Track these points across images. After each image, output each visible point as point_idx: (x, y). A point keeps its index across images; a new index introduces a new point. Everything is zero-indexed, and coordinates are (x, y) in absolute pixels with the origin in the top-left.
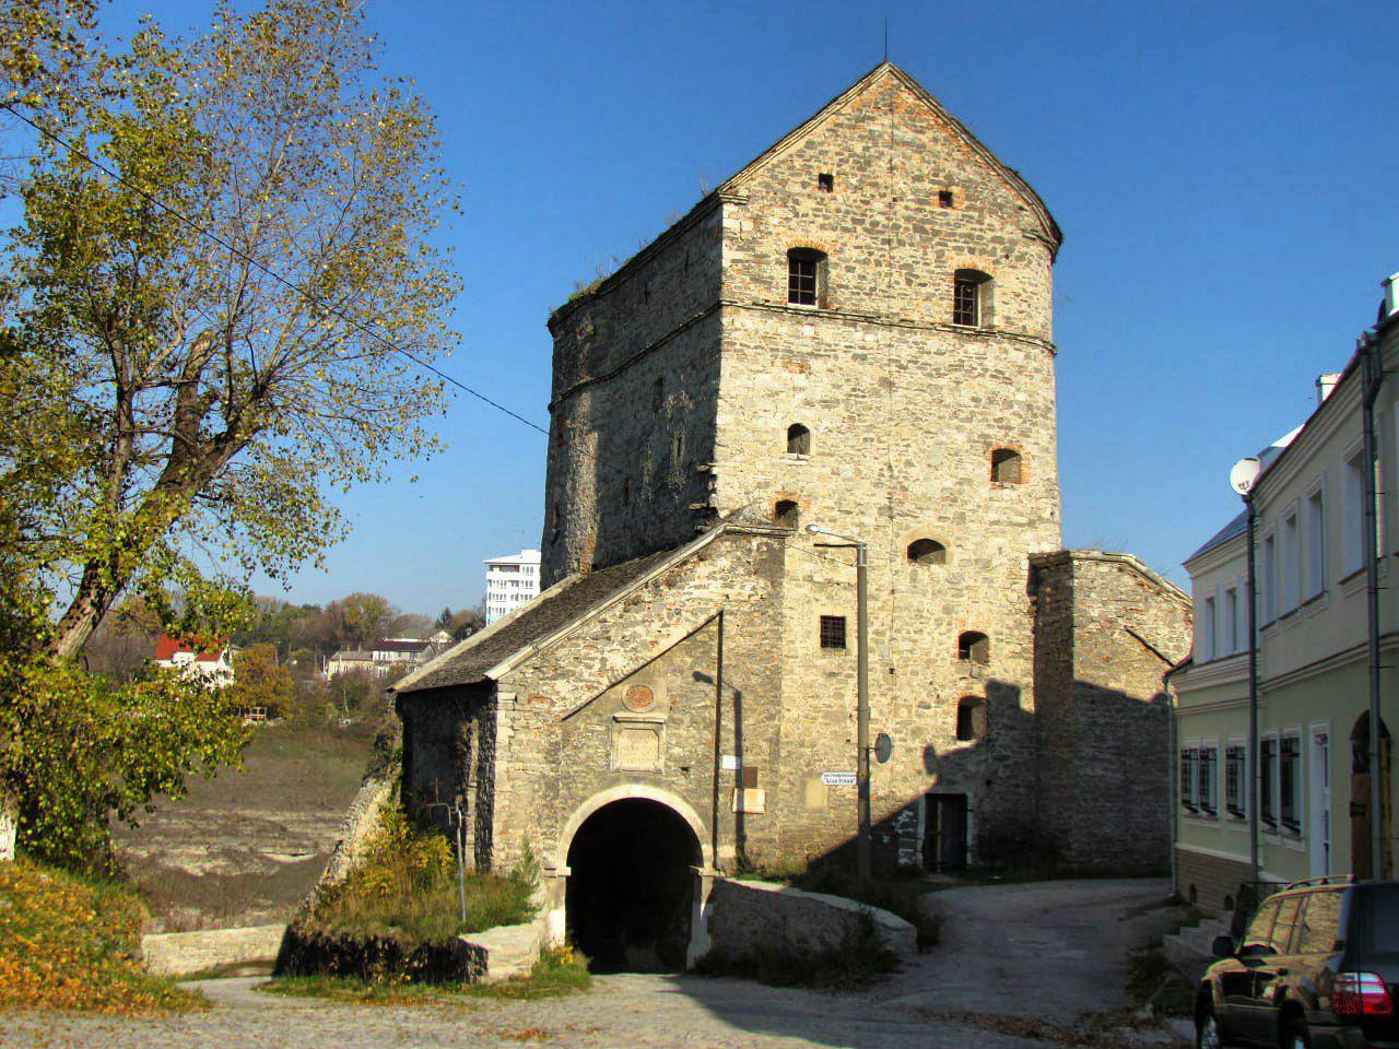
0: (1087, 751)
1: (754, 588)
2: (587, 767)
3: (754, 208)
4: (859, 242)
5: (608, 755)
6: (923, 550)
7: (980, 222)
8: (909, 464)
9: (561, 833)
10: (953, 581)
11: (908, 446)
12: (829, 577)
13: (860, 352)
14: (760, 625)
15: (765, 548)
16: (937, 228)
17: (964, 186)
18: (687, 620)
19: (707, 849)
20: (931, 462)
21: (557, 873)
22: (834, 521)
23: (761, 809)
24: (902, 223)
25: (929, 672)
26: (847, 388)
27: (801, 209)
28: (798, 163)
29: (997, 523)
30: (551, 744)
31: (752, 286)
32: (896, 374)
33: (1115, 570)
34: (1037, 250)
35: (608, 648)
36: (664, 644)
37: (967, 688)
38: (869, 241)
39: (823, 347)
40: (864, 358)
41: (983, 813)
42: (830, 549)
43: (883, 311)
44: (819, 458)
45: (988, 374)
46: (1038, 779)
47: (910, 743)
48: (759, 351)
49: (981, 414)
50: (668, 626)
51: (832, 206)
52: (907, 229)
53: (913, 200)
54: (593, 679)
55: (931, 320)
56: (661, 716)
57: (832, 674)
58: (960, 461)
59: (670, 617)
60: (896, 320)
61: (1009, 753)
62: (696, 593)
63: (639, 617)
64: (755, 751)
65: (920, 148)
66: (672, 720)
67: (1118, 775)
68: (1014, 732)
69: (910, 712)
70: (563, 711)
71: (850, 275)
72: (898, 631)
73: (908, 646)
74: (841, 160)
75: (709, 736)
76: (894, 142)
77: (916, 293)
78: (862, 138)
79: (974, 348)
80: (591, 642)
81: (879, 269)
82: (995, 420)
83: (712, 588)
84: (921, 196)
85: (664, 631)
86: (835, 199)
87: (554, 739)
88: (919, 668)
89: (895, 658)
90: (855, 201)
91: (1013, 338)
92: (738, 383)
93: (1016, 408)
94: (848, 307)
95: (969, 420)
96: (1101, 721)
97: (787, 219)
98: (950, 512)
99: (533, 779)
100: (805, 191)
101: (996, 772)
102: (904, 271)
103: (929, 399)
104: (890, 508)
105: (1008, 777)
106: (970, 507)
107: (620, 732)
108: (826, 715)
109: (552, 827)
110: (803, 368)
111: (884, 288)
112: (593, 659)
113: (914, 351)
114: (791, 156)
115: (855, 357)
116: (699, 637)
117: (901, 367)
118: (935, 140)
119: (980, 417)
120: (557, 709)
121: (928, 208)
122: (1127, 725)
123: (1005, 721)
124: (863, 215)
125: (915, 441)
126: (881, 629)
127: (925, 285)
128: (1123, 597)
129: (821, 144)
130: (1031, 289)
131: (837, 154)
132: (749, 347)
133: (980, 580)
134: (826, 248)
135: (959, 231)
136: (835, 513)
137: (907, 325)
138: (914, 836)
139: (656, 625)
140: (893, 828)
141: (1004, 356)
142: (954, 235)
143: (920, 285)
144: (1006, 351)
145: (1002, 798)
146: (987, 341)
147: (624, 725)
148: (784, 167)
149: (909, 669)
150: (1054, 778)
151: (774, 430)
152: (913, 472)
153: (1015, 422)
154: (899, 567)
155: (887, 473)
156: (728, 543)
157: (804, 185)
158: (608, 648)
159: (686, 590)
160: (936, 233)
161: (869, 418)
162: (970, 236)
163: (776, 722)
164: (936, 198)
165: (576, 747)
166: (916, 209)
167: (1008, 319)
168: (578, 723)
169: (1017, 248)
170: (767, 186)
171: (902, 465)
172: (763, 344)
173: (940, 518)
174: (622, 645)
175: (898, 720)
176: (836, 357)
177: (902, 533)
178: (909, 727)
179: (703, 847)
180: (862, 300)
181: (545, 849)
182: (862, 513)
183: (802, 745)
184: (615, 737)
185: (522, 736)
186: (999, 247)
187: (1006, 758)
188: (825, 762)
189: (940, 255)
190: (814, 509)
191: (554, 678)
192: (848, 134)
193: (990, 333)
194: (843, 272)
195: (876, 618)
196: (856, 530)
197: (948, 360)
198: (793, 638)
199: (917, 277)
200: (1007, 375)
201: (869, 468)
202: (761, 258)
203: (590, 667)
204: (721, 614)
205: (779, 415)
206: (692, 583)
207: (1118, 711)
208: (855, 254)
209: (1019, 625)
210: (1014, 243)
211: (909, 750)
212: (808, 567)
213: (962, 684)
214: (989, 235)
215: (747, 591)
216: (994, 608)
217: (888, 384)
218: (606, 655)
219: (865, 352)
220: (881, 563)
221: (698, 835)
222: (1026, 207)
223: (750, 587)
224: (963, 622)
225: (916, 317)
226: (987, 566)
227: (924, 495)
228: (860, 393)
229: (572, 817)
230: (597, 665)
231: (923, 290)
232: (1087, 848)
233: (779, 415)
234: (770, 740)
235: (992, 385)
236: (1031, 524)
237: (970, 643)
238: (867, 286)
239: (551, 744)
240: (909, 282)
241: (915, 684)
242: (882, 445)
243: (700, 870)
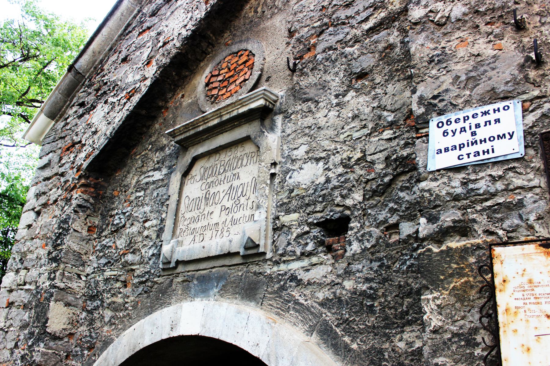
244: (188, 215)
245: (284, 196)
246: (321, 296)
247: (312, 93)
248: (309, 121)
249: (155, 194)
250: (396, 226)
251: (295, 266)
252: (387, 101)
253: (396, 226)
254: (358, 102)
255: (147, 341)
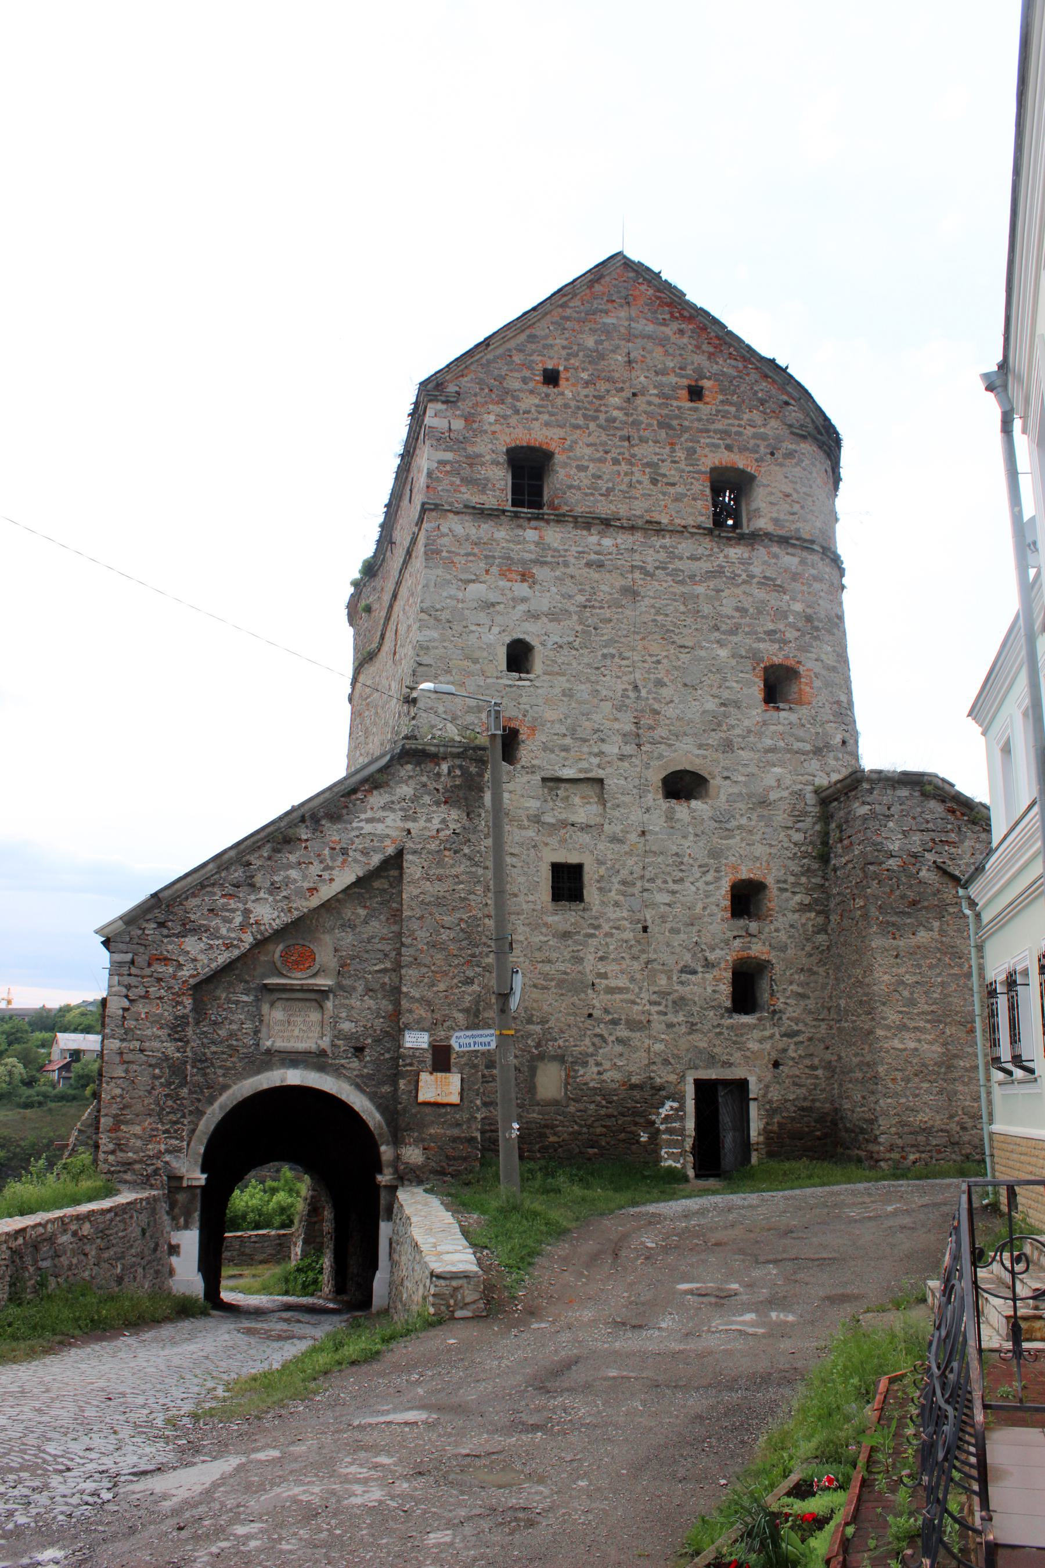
0: (892, 1017)
1: (443, 821)
2: (230, 1046)
3: (465, 406)
4: (591, 440)
5: (256, 1032)
6: (682, 786)
7: (736, 418)
8: (660, 683)
9: (193, 1131)
10: (720, 820)
11: (658, 662)
12: (563, 816)
13: (593, 557)
14: (452, 866)
15: (458, 772)
16: (686, 423)
17: (716, 381)
18: (355, 861)
19: (386, 1151)
20: (688, 681)
21: (185, 1184)
22: (566, 749)
23: (455, 1099)
24: (643, 418)
25: (695, 929)
26: (581, 599)
27: (522, 406)
28: (517, 359)
29: (772, 750)
30: (176, 1018)
31: (463, 489)
32: (641, 582)
33: (917, 794)
34: (807, 448)
35: (253, 897)
36: (327, 892)
37: (743, 949)
38: (604, 438)
39: (550, 553)
40: (600, 565)
41: (770, 1102)
42: (563, 785)
43: (623, 511)
44: (547, 677)
45: (755, 580)
46: (840, 1058)
47: (671, 1018)
48: (470, 558)
49: (749, 625)
50: (332, 868)
51: (559, 401)
52: (651, 425)
53: (657, 395)
54: (233, 935)
55: (683, 523)
56: (324, 982)
57: (566, 935)
58: (725, 679)
59: (332, 858)
60: (640, 523)
61: (801, 1027)
62: (368, 828)
63: (293, 858)
64: (446, 1024)
65: (662, 342)
66: (340, 986)
67: (934, 1048)
68: (808, 1002)
69: (669, 978)
70: (192, 976)
71: (583, 474)
72: (651, 880)
73: (666, 898)
74: (568, 354)
75: (386, 1005)
76: (630, 337)
77: (664, 494)
78: (593, 331)
79: (735, 552)
80: (230, 889)
81: (616, 468)
82: (765, 632)
83: (389, 822)
84: (666, 390)
85: (326, 875)
86: (562, 394)
87: (180, 1011)
88: (680, 925)
89: (649, 915)
90: (586, 396)
91: (784, 541)
92: (445, 594)
93: (791, 619)
94: (579, 510)
95: (733, 632)
96: (909, 979)
97: (505, 417)
98: (714, 738)
99: (153, 1061)
100: (526, 387)
101: (785, 1050)
102: (647, 470)
103: (682, 608)
104: (638, 735)
105: (800, 1056)
106: (737, 731)
107: (272, 1004)
108: (560, 984)
109: (175, 1123)
110: (525, 577)
111: (624, 487)
112: (233, 911)
113: (662, 556)
114: (509, 350)
115: (589, 565)
116: (377, 884)
117: (647, 574)
118: (681, 332)
119: (747, 629)
120: (185, 973)
121: (675, 403)
122: (943, 984)
123: (794, 987)
124: (597, 411)
125: (667, 657)
126: (630, 878)
127: (673, 485)
128: (930, 826)
129: (546, 337)
130: (804, 489)
131: (564, 348)
132: (458, 554)
133: (754, 817)
134: (553, 447)
135: (712, 427)
136: (568, 741)
137: (654, 528)
138: (682, 1131)
139: (315, 869)
140: (654, 1123)
141: (774, 561)
142: (708, 431)
143: (667, 484)
144: (776, 556)
145: (795, 1084)
146: (752, 545)
147: (277, 995)
148: (500, 363)
149: (668, 926)
150: (856, 1055)
151: (489, 645)
152: (665, 692)
153: (791, 634)
154: (651, 803)
155: (632, 694)
156: (409, 767)
157: (525, 381)
158: (253, 897)
159: (355, 825)
160: (684, 429)
161: (607, 631)
162: (725, 433)
163: (476, 987)
164: (684, 393)
165: (215, 1023)
166: (660, 405)
167: (776, 521)
168: (218, 993)
169: (784, 445)
170: (480, 382)
171: (651, 685)
172: (476, 551)
173: (700, 746)
174: (271, 894)
175: (657, 989)
176: (566, 565)
177: (655, 763)
178: (670, 998)
179: (383, 1148)
180: (598, 501)
181: (168, 1151)
182: (603, 740)
183: (530, 1021)
184: (265, 1008)
185: (141, 1008)
186: (763, 445)
187: (797, 1033)
188: (561, 1042)
189: (691, 452)
190: (541, 737)
191: (182, 935)
192: (577, 327)
193: (754, 538)
194: (573, 471)
195: (624, 865)
196: (595, 761)
197: (705, 566)
198: (516, 890)
199: (664, 476)
200: (778, 582)
201: (609, 688)
202: (473, 460)
203: (227, 921)
204: (400, 854)
205: (496, 630)
206: (363, 816)
207: (931, 967)
208: (588, 451)
209: (808, 872)
210: (779, 439)
211: (670, 1025)
212: (533, 804)
213: (737, 943)
214: (750, 431)
215: (436, 823)
216: (773, 851)
217: (631, 593)
218: (250, 905)
219: (602, 558)
220: (627, 799)
221: (376, 1132)
222: (793, 402)
223: (438, 820)
224: (735, 868)
225: (665, 520)
226: (764, 803)
227: (679, 719)
228: (597, 604)
229: (208, 1112)
230: (238, 919)
231: (672, 490)
232: (899, 1142)
233: (496, 630)
234: (466, 1011)
235: (760, 594)
236: (817, 751)
237: (745, 899)
238: (604, 486)
239: (176, 1018)
240: (654, 482)
241: (676, 944)
242: (624, 663)
243: (379, 1178)
244: (276, 1028)
245: (336, 1032)
246: (355, 1073)
247: (349, 989)
248: (347, 1002)
249: (246, 1009)
250: (383, 1054)
251: (343, 1061)
252: (382, 1007)
253: (383, 1054)
254: (370, 1002)
255: (265, 1086)
